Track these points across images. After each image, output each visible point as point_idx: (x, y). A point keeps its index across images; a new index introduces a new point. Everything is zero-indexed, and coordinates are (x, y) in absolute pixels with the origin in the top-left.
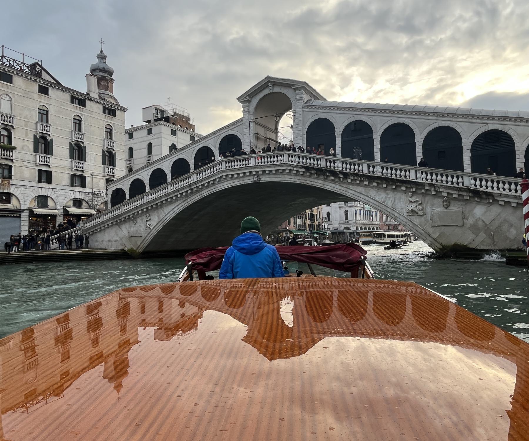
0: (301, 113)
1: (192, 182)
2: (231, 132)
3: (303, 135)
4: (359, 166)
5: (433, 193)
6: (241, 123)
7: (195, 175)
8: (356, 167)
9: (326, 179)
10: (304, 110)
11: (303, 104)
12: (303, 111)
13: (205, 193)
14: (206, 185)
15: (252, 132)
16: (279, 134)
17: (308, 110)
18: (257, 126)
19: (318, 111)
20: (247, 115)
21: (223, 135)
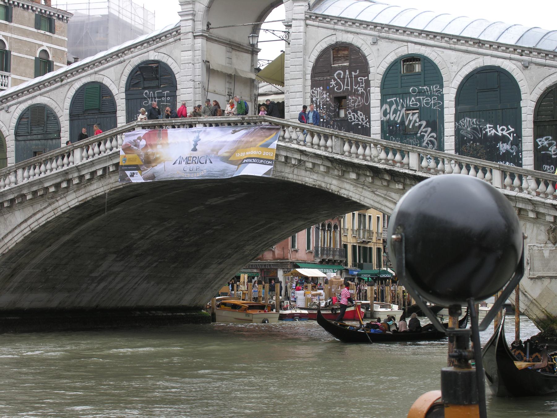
0: (302, 29)
1: (71, 165)
2: (153, 56)
3: (305, 74)
4: (403, 157)
5: (532, 215)
6: (178, 37)
7: (77, 153)
8: (398, 157)
9: (340, 178)
10: (308, 22)
11: (307, 8)
12: (307, 25)
13: (98, 189)
14: (100, 173)
15: (199, 58)
16: (260, 56)
17: (316, 23)
18: (209, 43)
19: (336, 27)
20: (190, 23)
21: (136, 61)
